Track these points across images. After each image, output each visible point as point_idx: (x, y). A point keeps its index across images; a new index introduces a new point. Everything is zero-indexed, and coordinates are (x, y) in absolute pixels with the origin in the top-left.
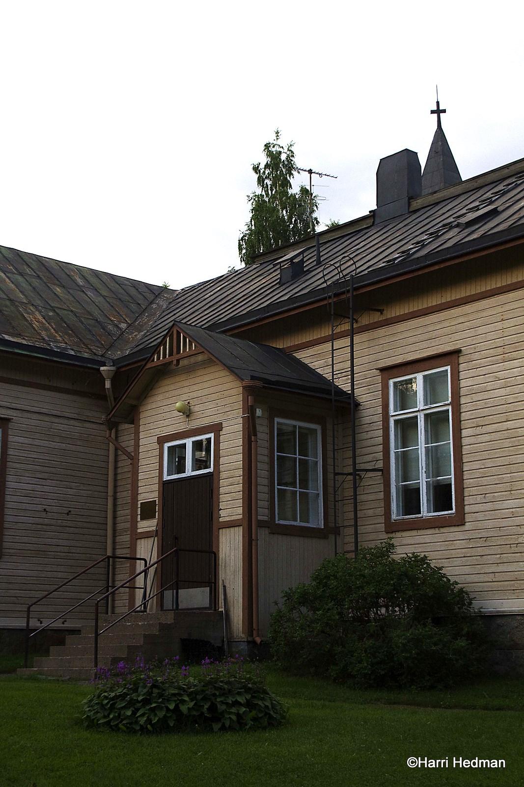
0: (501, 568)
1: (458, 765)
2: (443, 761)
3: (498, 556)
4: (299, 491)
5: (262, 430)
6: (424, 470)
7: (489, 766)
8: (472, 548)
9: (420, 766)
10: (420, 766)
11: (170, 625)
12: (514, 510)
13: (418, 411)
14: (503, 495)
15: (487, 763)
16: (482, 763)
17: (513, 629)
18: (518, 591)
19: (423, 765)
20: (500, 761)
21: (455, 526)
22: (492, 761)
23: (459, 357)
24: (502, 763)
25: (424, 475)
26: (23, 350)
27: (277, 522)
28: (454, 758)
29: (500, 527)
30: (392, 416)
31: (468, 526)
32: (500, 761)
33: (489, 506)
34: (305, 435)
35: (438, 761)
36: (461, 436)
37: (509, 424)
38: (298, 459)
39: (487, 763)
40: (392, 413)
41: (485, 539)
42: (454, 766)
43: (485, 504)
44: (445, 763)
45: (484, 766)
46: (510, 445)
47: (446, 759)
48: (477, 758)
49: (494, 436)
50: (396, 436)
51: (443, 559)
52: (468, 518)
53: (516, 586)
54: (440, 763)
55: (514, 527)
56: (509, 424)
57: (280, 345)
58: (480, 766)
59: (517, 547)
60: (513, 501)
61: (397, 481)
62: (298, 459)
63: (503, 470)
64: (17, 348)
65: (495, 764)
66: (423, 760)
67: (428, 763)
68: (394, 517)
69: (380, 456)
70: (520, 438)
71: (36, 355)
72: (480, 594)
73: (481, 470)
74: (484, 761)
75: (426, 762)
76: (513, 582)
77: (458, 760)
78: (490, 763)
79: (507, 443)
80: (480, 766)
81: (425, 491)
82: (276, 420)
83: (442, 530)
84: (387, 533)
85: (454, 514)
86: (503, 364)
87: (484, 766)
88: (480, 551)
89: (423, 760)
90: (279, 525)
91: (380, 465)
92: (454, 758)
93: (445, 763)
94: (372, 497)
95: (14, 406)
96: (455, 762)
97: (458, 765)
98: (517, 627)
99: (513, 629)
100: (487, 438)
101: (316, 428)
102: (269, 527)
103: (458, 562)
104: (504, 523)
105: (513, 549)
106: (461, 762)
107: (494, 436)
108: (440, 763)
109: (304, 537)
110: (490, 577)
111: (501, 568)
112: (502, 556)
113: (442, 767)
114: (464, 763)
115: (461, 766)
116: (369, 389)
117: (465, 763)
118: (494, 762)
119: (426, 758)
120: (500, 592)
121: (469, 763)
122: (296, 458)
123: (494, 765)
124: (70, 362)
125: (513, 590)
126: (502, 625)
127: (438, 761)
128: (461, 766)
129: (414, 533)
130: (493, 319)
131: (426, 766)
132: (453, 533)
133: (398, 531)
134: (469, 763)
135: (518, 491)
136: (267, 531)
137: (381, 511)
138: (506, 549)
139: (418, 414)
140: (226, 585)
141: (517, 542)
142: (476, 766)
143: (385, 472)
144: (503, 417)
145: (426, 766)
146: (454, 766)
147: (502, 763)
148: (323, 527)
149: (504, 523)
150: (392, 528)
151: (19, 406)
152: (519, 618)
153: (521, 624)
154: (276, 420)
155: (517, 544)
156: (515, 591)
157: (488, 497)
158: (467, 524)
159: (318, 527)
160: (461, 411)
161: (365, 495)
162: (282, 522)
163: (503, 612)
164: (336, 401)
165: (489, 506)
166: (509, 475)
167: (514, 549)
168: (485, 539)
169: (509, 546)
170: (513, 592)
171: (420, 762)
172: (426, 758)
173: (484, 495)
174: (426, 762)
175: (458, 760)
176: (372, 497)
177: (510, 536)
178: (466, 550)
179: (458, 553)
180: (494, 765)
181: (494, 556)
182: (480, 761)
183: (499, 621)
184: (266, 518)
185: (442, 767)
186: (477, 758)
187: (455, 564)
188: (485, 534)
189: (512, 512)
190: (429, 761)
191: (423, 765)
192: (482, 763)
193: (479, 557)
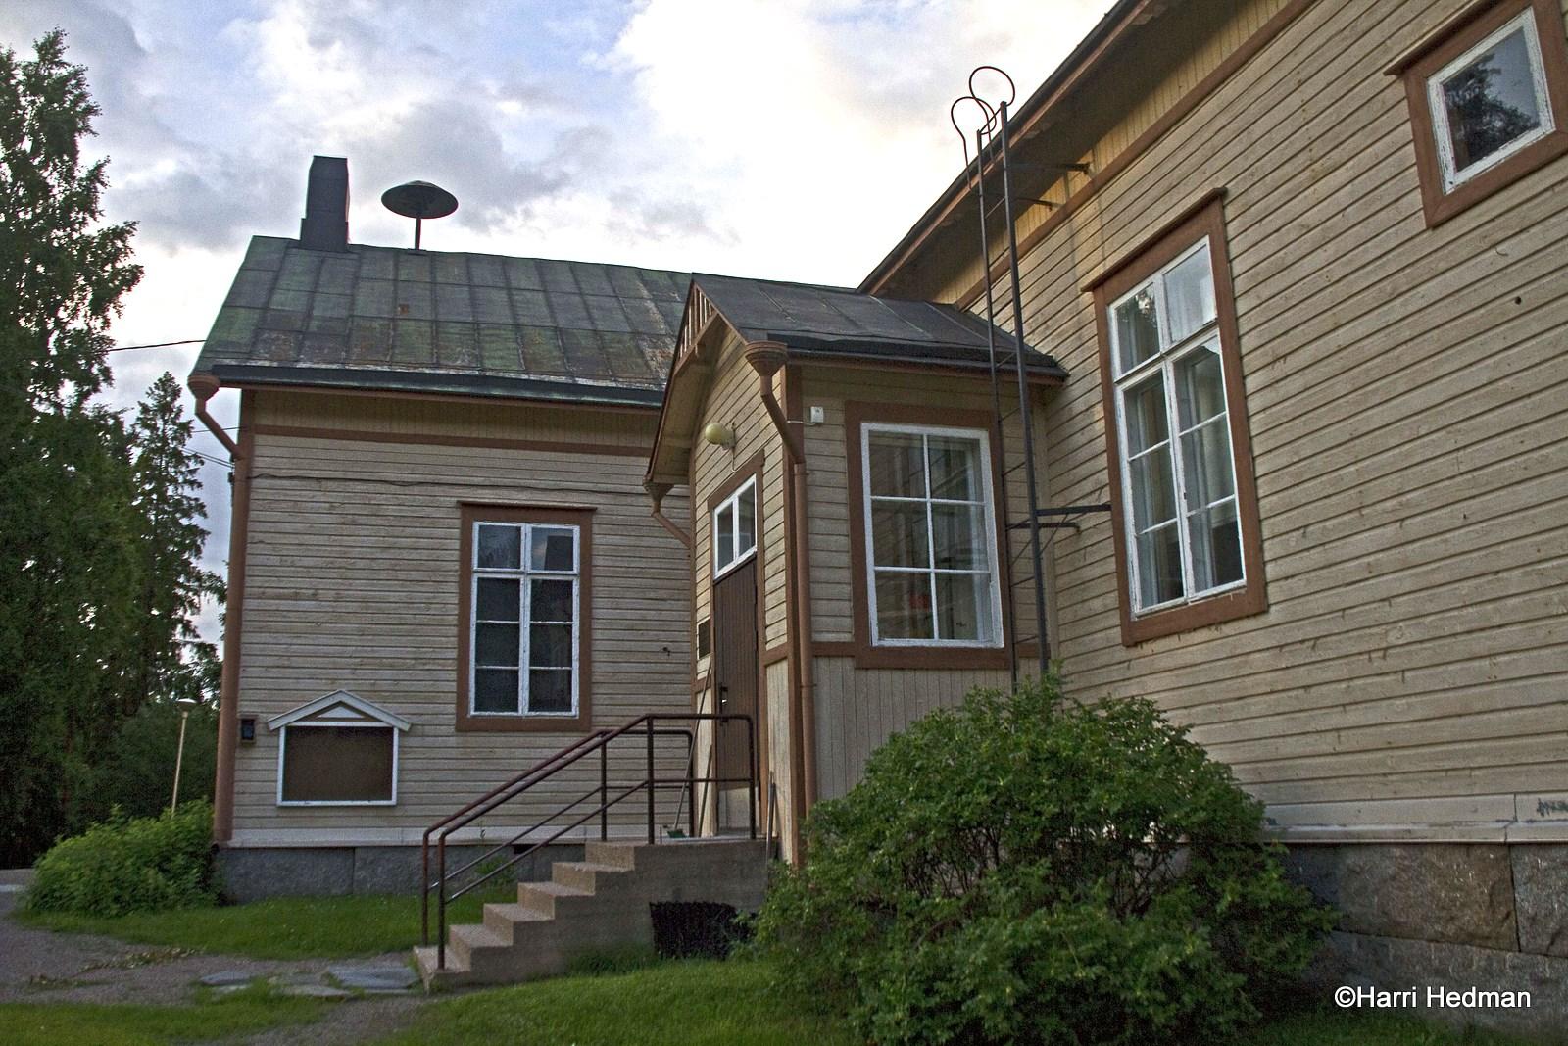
0: (1353, 717)
1: (1436, 1001)
2: (1405, 994)
3: (1343, 686)
4: (936, 574)
5: (826, 456)
6: (1183, 490)
7: (1497, 1005)
8: (1287, 668)
9: (1360, 1005)
10: (1360, 1005)
11: (624, 875)
12: (1371, 558)
13: (1162, 358)
14: (1344, 523)
15: (1493, 997)
16: (1485, 997)
17: (1385, 881)
18: (1394, 778)
19: (1366, 1001)
20: (1520, 995)
21: (1248, 616)
22: (1504, 995)
23: (1224, 207)
24: (1524, 997)
25: (1184, 502)
26: (597, 396)
27: (876, 643)
28: (1429, 989)
29: (1344, 609)
30: (1120, 382)
31: (1275, 614)
32: (1520, 995)
33: (1316, 557)
34: (953, 460)
35: (1396, 994)
36: (1245, 392)
37: (1342, 336)
38: (929, 505)
39: (1493, 997)
40: (1118, 376)
41: (1312, 643)
42: (1429, 1005)
43: (1306, 553)
44: (1410, 998)
45: (1489, 1005)
46: (1350, 388)
47: (1412, 991)
48: (1474, 989)
49: (1312, 376)
50: (1130, 426)
51: (1230, 700)
52: (1274, 593)
53: (1389, 762)
54: (1400, 998)
55: (1374, 605)
56: (1342, 336)
57: (950, 298)
58: (1480, 1005)
59: (1384, 657)
60: (1366, 535)
61: (1138, 527)
62: (929, 505)
63: (1340, 456)
64: (588, 395)
65: (1510, 1000)
66: (1366, 991)
67: (1376, 999)
68: (1137, 608)
69: (1104, 477)
70: (1369, 364)
71: (620, 401)
72: (1309, 788)
73: (1293, 467)
74: (1489, 995)
75: (1372, 996)
76: (1379, 755)
77: (1436, 992)
78: (1501, 999)
79: (1341, 386)
80: (1480, 1005)
81: (1187, 540)
82: (866, 428)
83: (1227, 629)
84: (1128, 647)
85: (1244, 587)
86: (1312, 188)
87: (1489, 1005)
88: (1303, 676)
89: (1366, 991)
90: (882, 648)
91: (1106, 497)
92: (1429, 989)
93: (1410, 998)
94: (1097, 571)
95: (603, 487)
96: (1430, 996)
97: (1436, 1001)
98: (1393, 878)
99: (1385, 881)
100: (1296, 384)
101: (976, 437)
102: (852, 656)
103: (1258, 706)
104: (1352, 596)
105: (1376, 664)
106: (1441, 996)
107: (1312, 376)
108: (1400, 998)
109: (950, 669)
110: (1326, 743)
111: (1353, 717)
112: (1352, 684)
113: (1405, 1005)
114: (1449, 999)
115: (1442, 1005)
116: (1059, 335)
117: (1451, 999)
118: (1509, 996)
119: (1372, 989)
120: (1353, 779)
121: (1459, 998)
122: (925, 503)
123: (1507, 1003)
124: (596, 400)
125: (1384, 775)
126: (1358, 869)
127: (1396, 994)
128: (1442, 1005)
129: (1172, 642)
130: (1282, 90)
131: (1372, 1005)
132: (1244, 634)
133: (1147, 641)
134: (1459, 998)
135: (1378, 507)
136: (848, 664)
137: (1112, 600)
138: (1360, 665)
139: (1161, 365)
140: (778, 783)
141: (1384, 645)
142: (1473, 1004)
143: (1114, 507)
144: (1326, 322)
145: (1372, 1005)
146: (1429, 1005)
147: (1524, 997)
148: (1003, 646)
149: (1352, 596)
150: (1137, 634)
151: (611, 488)
152: (1398, 852)
153: (1404, 870)
154: (866, 428)
155: (1385, 649)
156: (1390, 778)
157: (1312, 533)
158: (1273, 609)
159: (989, 645)
160: (1241, 333)
161: (1088, 568)
162: (889, 642)
163: (1359, 835)
164: (998, 370)
165: (1316, 557)
166: (1353, 468)
167: (1378, 664)
168: (1312, 643)
169: (1366, 656)
170: (1381, 779)
171: (1360, 996)
172: (1372, 989)
173: (1302, 531)
174: (1372, 996)
175: (1436, 992)
176: (1097, 571)
177: (1368, 631)
178: (1273, 675)
179: (1258, 685)
180: (1507, 1003)
181: (1334, 686)
182: (1481, 994)
183: (1352, 859)
184: (846, 638)
185: (1405, 1005)
186: (1474, 989)
187: (1254, 710)
188: (1311, 631)
189: (1369, 564)
190: (1379, 995)
191: (1366, 1001)
192: (1485, 997)
193: (1302, 691)
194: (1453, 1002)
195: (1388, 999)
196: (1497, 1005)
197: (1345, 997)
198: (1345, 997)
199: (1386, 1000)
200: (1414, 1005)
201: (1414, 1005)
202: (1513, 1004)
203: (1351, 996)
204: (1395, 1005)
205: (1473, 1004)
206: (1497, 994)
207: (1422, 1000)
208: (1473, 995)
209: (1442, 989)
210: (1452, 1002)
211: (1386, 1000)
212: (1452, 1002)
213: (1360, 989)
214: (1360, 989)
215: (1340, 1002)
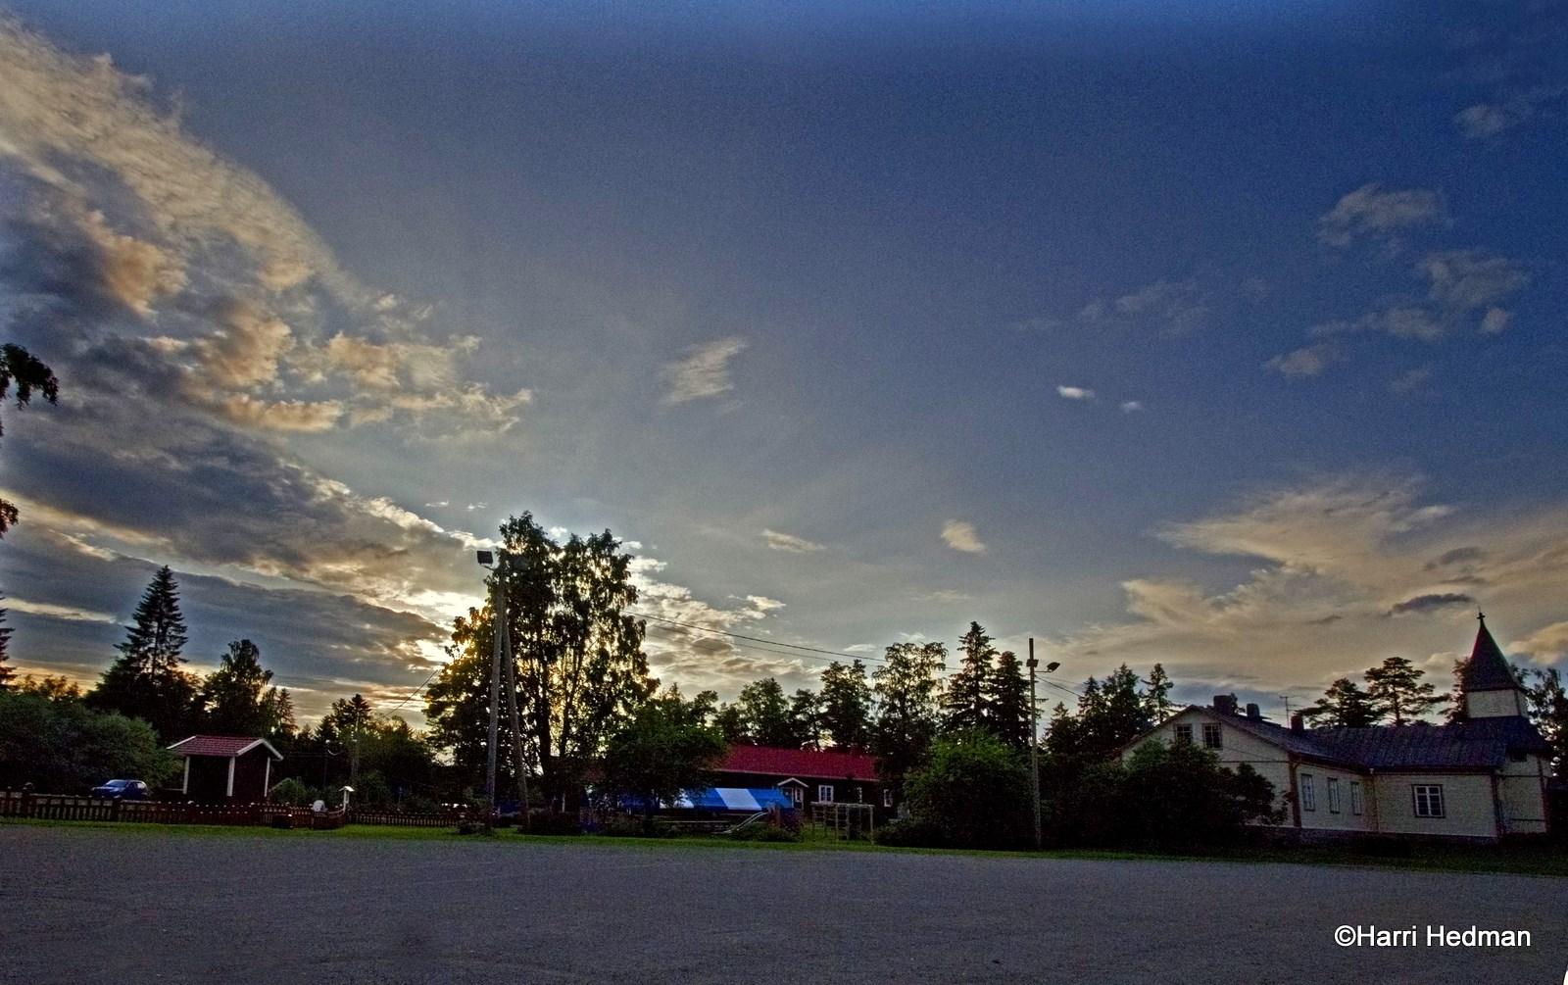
1: (1435, 940)
2: (1405, 933)
7: (1497, 944)
9: (1360, 944)
10: (1360, 944)
15: (1493, 936)
16: (1485, 936)
19: (1366, 940)
20: (1520, 934)
22: (1504, 934)
24: (1524, 936)
28: (1429, 928)
32: (1520, 934)
35: (1396, 933)
39: (1493, 936)
42: (1429, 944)
44: (1409, 937)
45: (1489, 944)
47: (1412, 930)
48: (1474, 928)
54: (1400, 937)
58: (1480, 944)
65: (1510, 939)
66: (1366, 930)
67: (1376, 938)
74: (1489, 934)
75: (1372, 935)
77: (1435, 930)
78: (1501, 938)
80: (1480, 944)
87: (1489, 944)
89: (1366, 930)
92: (1429, 928)
93: (1409, 937)
96: (1430, 935)
97: (1435, 940)
106: (1441, 935)
108: (1400, 937)
113: (1405, 944)
114: (1449, 938)
115: (1442, 944)
117: (1451, 938)
118: (1508, 935)
119: (1372, 928)
121: (1459, 937)
123: (1507, 941)
127: (1396, 933)
128: (1442, 944)
131: (1372, 944)
134: (1459, 937)
142: (1473, 943)
145: (1372, 944)
146: (1429, 944)
147: (1524, 936)
171: (1360, 935)
172: (1372, 928)
174: (1372, 935)
175: (1435, 930)
180: (1507, 941)
182: (1481, 934)
185: (1405, 944)
186: (1474, 928)
190: (1379, 934)
191: (1366, 940)
192: (1485, 936)
194: (1453, 941)
195: (1388, 938)
197: (1345, 936)
198: (1345, 936)
199: (1386, 939)
200: (1414, 944)
201: (1414, 944)
202: (1513, 943)
203: (1351, 935)
204: (1395, 944)
205: (1473, 943)
206: (1496, 933)
207: (1422, 937)
209: (1442, 928)
210: (1452, 941)
211: (1386, 939)
212: (1452, 941)
213: (1360, 928)
214: (1360, 928)
215: (1340, 941)
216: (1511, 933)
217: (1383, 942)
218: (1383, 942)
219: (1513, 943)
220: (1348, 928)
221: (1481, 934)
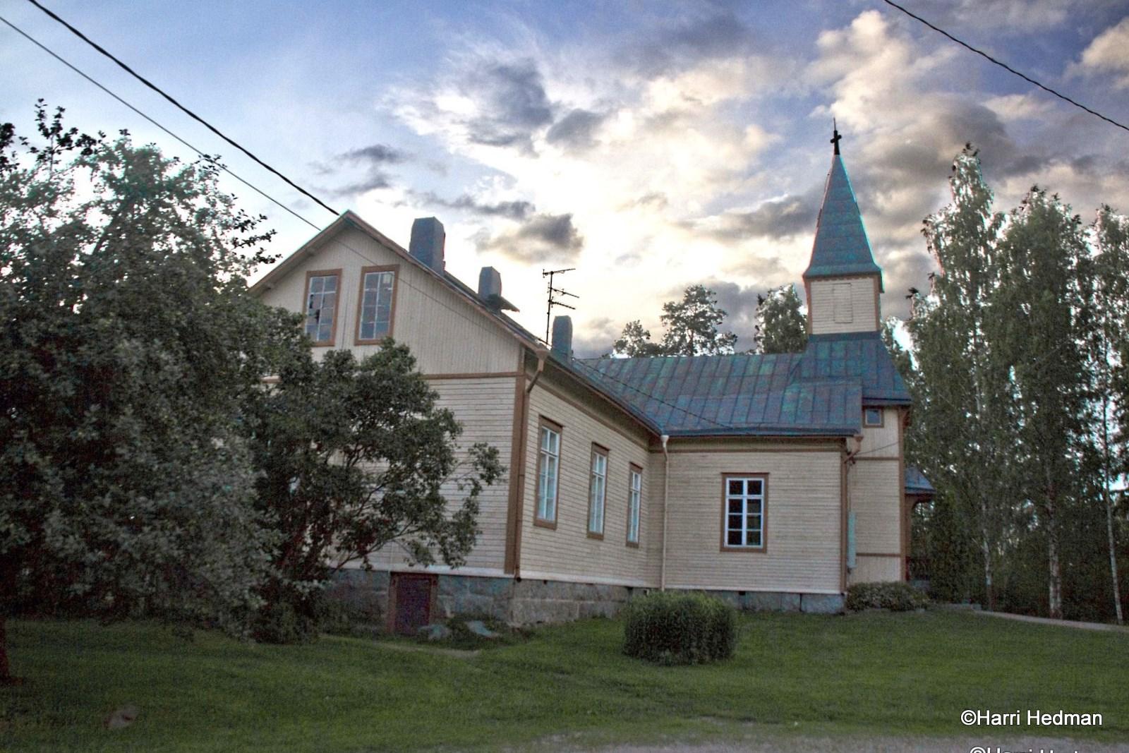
1: (1034, 721)
2: (1012, 716)
7: (1078, 724)
9: (979, 723)
10: (979, 723)
15: (1075, 718)
16: (1069, 718)
19: (984, 721)
20: (1095, 716)
24: (1098, 718)
28: (1029, 712)
32: (1095, 716)
35: (1005, 716)
39: (1075, 718)
42: (1029, 723)
44: (1015, 718)
45: (1072, 723)
47: (1017, 714)
48: (1061, 712)
54: (1008, 718)
58: (1066, 724)
66: (983, 714)
67: (991, 719)
74: (1072, 716)
75: (988, 717)
77: (1033, 714)
78: (1081, 719)
80: (1066, 724)
87: (1072, 723)
89: (983, 714)
92: (1029, 712)
93: (1015, 718)
96: (1029, 717)
97: (1034, 721)
106: (1038, 717)
108: (1008, 718)
114: (1043, 719)
115: (1038, 724)
119: (988, 712)
121: (1050, 719)
127: (1005, 716)
128: (1038, 724)
131: (988, 724)
134: (1050, 719)
142: (1061, 723)
145: (988, 724)
146: (1029, 723)
147: (1098, 718)
171: (979, 717)
172: (988, 712)
175: (1033, 714)
182: (1066, 716)
186: (1061, 712)
190: (993, 716)
191: (984, 721)
192: (1069, 718)
194: (1046, 721)
196: (1078, 724)
197: (969, 718)
198: (969, 718)
200: (1018, 724)
201: (1018, 724)
203: (973, 717)
204: (1005, 723)
207: (1024, 720)
208: (1061, 716)
209: (1038, 712)
210: (1046, 721)
212: (1046, 721)
213: (979, 712)
214: (979, 712)
215: (965, 721)
216: (1088, 715)
217: (996, 722)
218: (996, 722)
219: (1089, 723)
220: (971, 712)
221: (1066, 716)
